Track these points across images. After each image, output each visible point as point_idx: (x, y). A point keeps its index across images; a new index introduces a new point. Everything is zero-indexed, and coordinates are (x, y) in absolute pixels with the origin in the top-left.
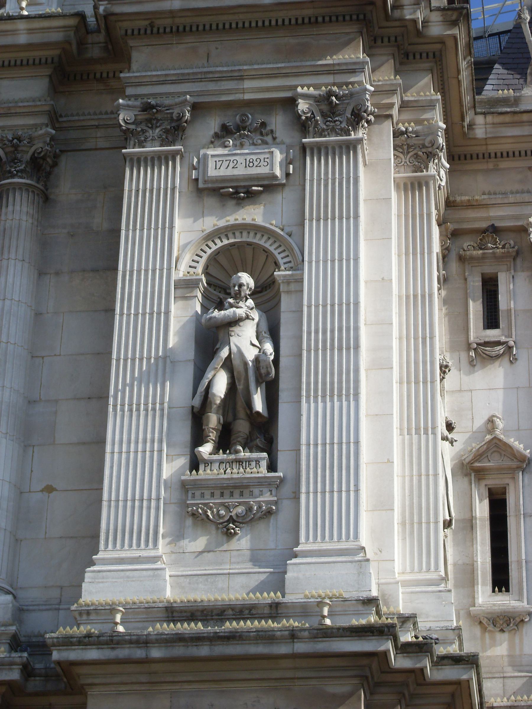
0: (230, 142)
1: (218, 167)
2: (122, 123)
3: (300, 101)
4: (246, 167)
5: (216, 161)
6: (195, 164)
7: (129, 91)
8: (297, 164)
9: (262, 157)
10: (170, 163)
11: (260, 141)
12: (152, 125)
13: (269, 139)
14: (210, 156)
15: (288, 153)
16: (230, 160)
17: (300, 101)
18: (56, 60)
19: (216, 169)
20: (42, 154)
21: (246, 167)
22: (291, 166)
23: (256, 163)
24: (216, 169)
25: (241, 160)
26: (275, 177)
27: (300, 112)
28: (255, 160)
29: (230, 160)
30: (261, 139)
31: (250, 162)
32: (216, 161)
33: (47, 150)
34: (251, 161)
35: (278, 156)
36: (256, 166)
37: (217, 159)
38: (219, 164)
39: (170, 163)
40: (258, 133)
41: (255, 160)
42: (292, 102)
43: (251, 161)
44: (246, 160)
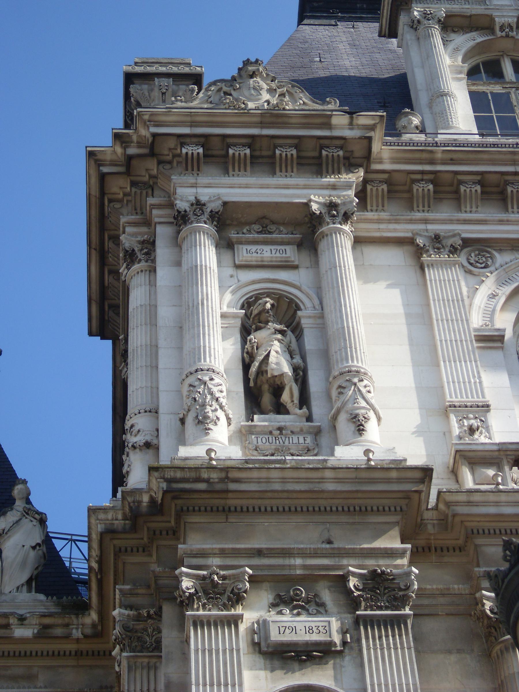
1: (282, 632)
4: (306, 633)
11: (315, 611)
15: (342, 624)
16: (286, 627)
19: (280, 633)
21: (306, 633)
26: (331, 644)
29: (286, 627)
30: (316, 609)
32: (279, 627)
34: (311, 628)
38: (282, 630)
40: (313, 603)
41: (314, 627)
42: (344, 579)
43: (311, 628)
44: (305, 627)
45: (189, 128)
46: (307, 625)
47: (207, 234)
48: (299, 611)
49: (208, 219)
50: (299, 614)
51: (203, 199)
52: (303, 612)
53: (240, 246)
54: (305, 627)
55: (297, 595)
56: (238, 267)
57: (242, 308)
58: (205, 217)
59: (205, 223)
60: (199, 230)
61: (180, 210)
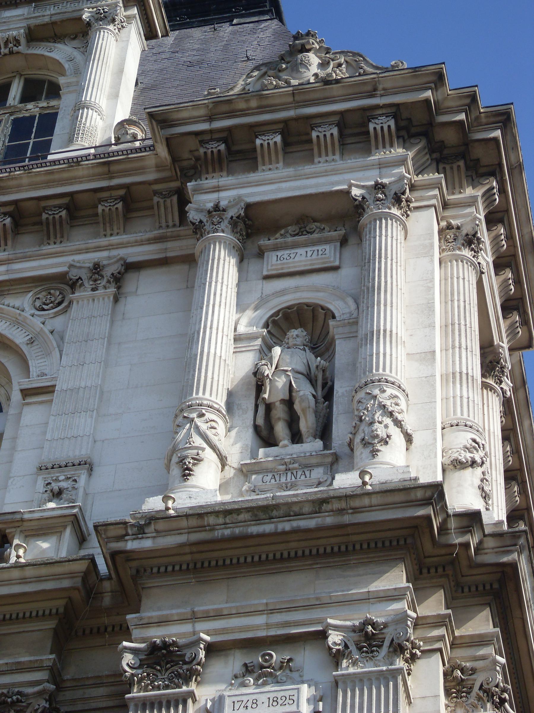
0: (250, 681)
2: (127, 669)
3: (330, 632)
4: (269, 706)
5: (234, 702)
6: (208, 707)
7: (136, 633)
8: (329, 700)
9: (287, 694)
10: (181, 707)
11: (284, 679)
12: (161, 668)
13: (295, 675)
14: (227, 698)
17: (330, 632)
18: (61, 610)
19: (234, 710)
20: (39, 711)
21: (269, 706)
22: (321, 704)
23: (280, 702)
24: (234, 710)
25: (263, 698)
27: (331, 645)
28: (279, 698)
31: (274, 701)
33: (45, 707)
35: (306, 692)
36: (281, 705)
37: (235, 699)
39: (181, 707)
41: (279, 698)
44: (269, 698)
45: (208, 124)
46: (272, 695)
47: (225, 242)
48: (264, 680)
49: (227, 227)
50: (264, 684)
51: (223, 204)
52: (269, 679)
53: (271, 253)
54: (269, 698)
55: (266, 661)
56: (267, 278)
57: (266, 326)
58: (225, 224)
59: (223, 231)
60: (215, 240)
61: (194, 221)
